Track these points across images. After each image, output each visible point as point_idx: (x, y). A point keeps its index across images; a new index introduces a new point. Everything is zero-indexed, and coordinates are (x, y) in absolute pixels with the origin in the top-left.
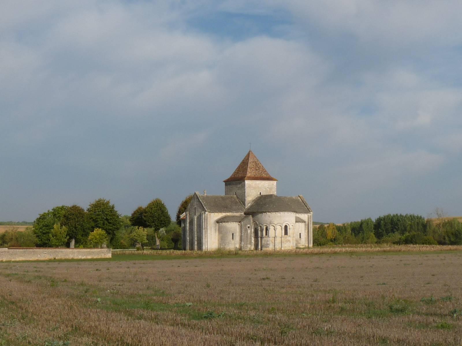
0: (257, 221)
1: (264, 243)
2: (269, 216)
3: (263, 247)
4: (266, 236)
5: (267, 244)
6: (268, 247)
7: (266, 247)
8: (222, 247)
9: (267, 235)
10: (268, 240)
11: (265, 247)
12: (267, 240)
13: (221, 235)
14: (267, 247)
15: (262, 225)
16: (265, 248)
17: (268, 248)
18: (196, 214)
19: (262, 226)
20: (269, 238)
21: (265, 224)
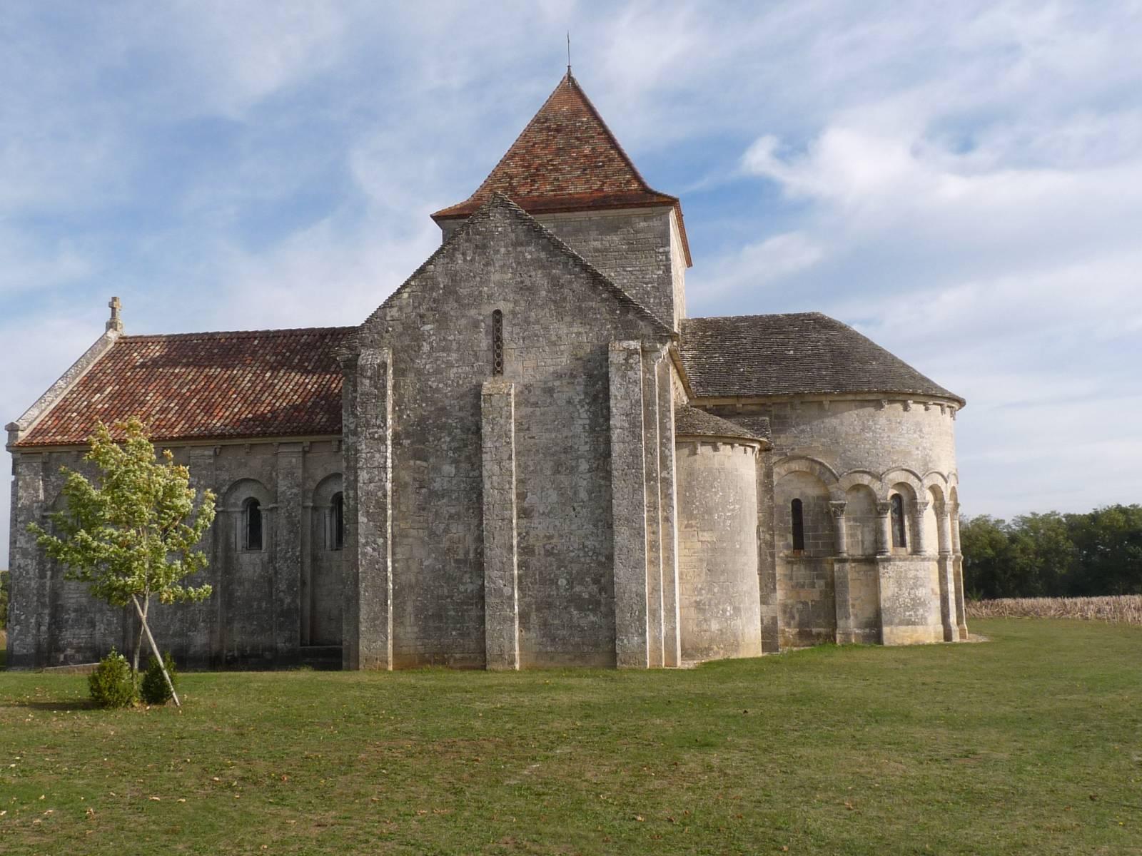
0: (828, 452)
1: (896, 597)
2: (918, 427)
3: (891, 623)
4: (902, 551)
5: (917, 603)
6: (922, 621)
7: (909, 623)
8: (715, 626)
9: (903, 544)
10: (921, 574)
11: (901, 623)
12: (916, 578)
13: (706, 536)
14: (914, 623)
15: (879, 477)
16: (903, 628)
17: (920, 628)
18: (512, 364)
19: (876, 486)
20: (926, 563)
21: (899, 477)
